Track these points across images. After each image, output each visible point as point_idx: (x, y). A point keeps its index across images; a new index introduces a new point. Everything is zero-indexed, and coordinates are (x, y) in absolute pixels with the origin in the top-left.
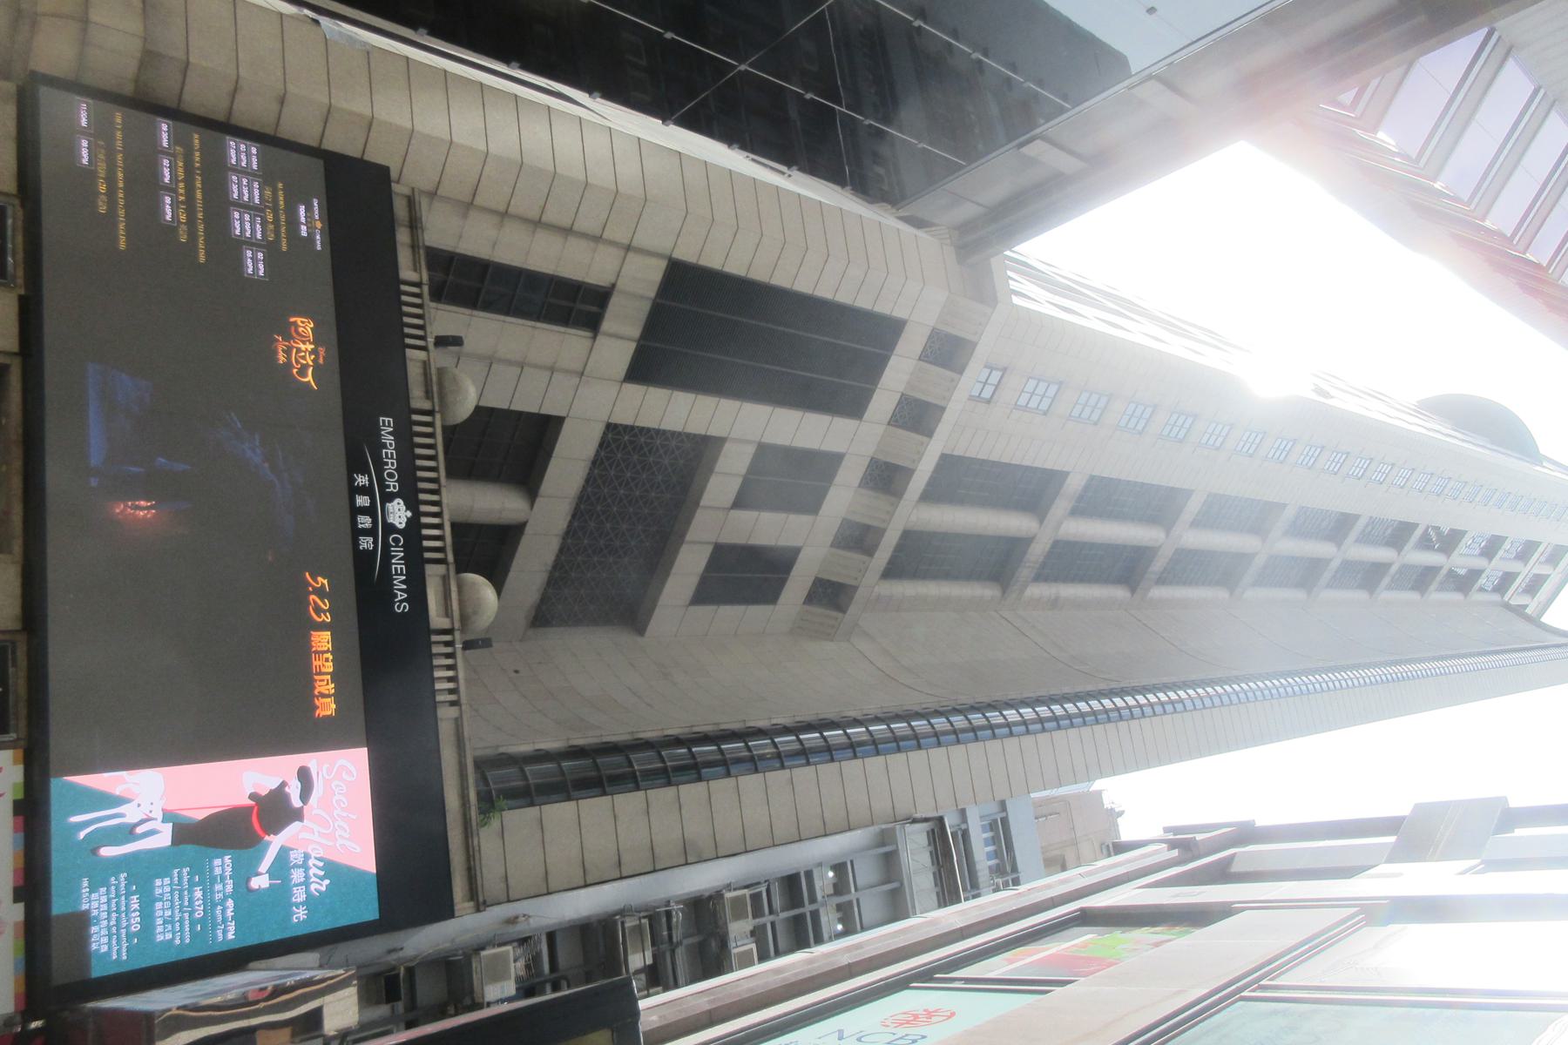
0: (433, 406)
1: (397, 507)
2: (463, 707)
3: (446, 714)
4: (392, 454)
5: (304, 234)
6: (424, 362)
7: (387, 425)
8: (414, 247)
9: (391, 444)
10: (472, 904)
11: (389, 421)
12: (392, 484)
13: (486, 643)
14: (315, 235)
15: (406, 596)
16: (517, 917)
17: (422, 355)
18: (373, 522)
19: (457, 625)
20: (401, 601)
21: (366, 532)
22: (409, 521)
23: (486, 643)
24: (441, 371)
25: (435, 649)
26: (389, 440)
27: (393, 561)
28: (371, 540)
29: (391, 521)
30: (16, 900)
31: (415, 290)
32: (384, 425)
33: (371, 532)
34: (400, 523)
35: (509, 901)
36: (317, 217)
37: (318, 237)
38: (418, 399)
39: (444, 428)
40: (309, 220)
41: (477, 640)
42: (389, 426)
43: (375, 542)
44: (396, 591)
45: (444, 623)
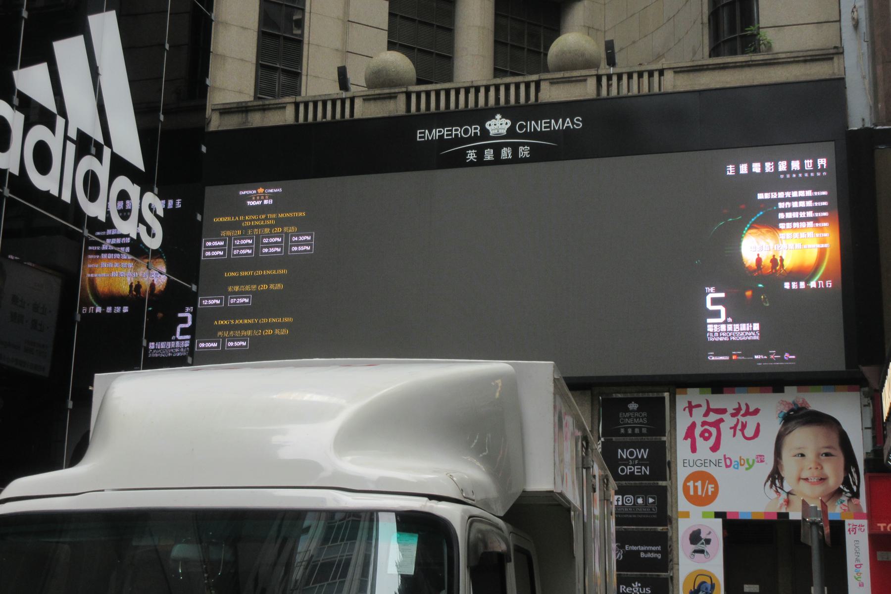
0: (402, 92)
1: (493, 127)
2: (664, 67)
3: (671, 83)
4: (447, 131)
5: (271, 202)
6: (364, 100)
7: (424, 135)
8: (264, 109)
9: (440, 132)
10: (836, 59)
11: (420, 133)
12: (473, 131)
13: (610, 46)
14: (270, 193)
15: (568, 119)
16: (853, 19)
17: (358, 103)
18: (507, 147)
19: (593, 72)
20: (573, 123)
21: (515, 152)
22: (504, 116)
23: (610, 46)
24: (371, 84)
25: (614, 92)
26: (436, 133)
27: (539, 130)
28: (521, 148)
29: (505, 131)
30: (782, 391)
31: (302, 108)
32: (424, 137)
33: (515, 148)
34: (507, 124)
35: (840, 21)
36: (254, 192)
37: (271, 191)
38: (397, 107)
39: (419, 82)
40: (258, 198)
41: (607, 54)
42: (424, 133)
43: (524, 144)
44: (564, 128)
45: (592, 83)
